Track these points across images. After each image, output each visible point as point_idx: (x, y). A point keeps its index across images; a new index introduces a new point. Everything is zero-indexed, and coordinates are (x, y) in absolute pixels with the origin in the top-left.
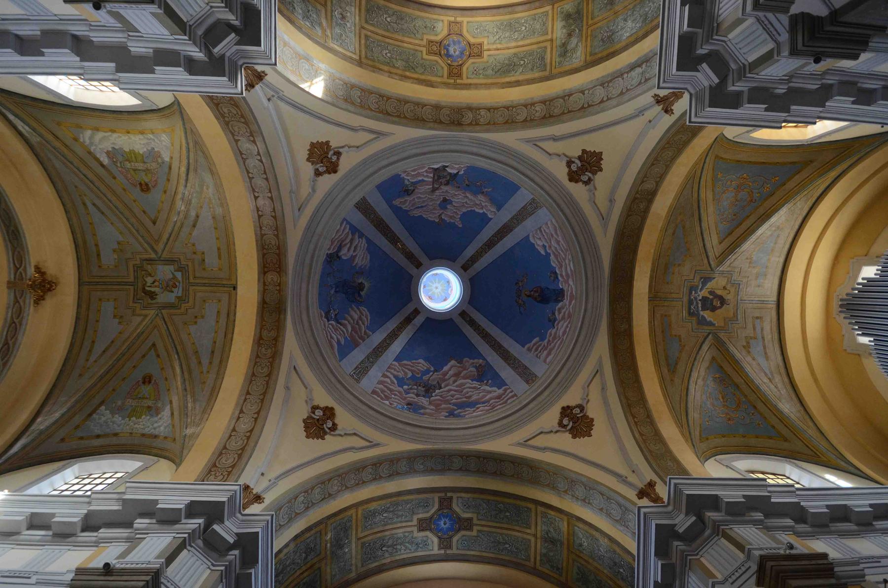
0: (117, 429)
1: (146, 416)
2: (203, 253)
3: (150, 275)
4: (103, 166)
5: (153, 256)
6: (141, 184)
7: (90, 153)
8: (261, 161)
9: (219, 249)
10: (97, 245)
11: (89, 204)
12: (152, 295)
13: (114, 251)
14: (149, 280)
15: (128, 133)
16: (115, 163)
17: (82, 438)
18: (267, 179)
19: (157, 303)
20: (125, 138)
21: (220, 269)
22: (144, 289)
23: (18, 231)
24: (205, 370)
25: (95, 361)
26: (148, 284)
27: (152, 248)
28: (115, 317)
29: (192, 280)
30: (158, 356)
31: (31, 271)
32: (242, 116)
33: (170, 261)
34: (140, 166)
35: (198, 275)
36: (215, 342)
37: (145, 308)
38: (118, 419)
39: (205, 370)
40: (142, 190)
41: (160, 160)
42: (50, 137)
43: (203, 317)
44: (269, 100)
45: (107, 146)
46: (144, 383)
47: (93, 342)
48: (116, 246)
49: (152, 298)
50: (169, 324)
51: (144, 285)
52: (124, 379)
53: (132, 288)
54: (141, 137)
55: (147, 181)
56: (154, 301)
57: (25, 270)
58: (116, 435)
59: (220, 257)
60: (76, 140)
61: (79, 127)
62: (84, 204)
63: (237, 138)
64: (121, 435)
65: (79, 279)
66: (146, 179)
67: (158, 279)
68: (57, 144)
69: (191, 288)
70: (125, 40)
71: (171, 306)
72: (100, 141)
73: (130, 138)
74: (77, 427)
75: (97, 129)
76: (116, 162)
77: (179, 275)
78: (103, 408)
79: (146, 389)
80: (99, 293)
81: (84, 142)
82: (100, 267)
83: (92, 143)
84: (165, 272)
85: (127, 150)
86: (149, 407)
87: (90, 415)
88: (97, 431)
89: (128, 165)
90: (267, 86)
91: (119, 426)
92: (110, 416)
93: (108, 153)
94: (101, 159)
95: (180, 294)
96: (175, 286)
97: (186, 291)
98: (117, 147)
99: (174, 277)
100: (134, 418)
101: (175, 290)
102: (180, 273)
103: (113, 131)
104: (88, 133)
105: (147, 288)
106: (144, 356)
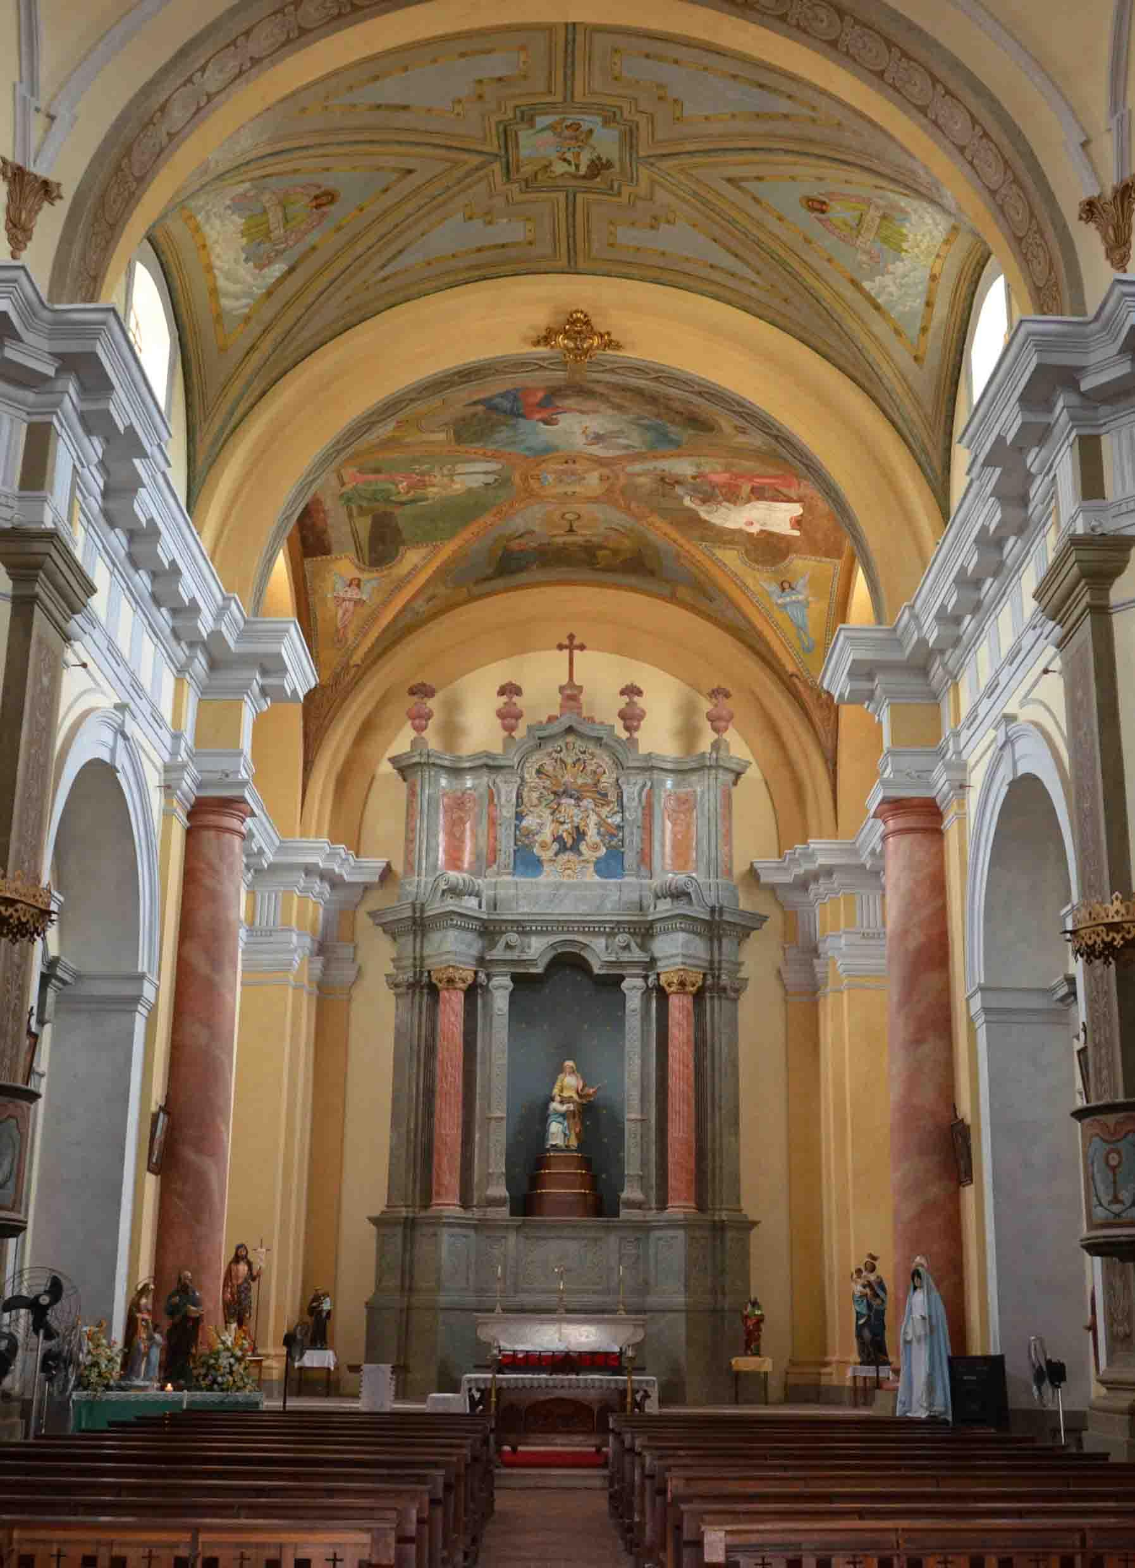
0: (920, 275)
1: (904, 226)
2: (480, 82)
3: (546, 167)
4: (292, 270)
5: (497, 166)
6: (318, 206)
7: (269, 293)
8: (203, 69)
9: (463, 55)
10: (479, 250)
11: (382, 274)
12: (598, 167)
13: (490, 223)
14: (560, 168)
15: (204, 246)
16: (279, 253)
17: (924, 330)
18: (247, 33)
19: (621, 159)
20: (218, 249)
21: (523, 48)
22: (584, 177)
23: (460, 372)
24: (806, 112)
25: (758, 273)
26: (572, 169)
27: (477, 169)
28: (652, 227)
29: (559, 98)
30: (759, 179)
31: (542, 350)
32: (119, 168)
33: (507, 137)
34: (274, 217)
35: (541, 86)
36: (735, 77)
37: (633, 179)
38: (899, 268)
39: (806, 112)
40: (332, 201)
41: (252, 193)
42: (255, 359)
43: (660, 86)
44: (52, 118)
45: (245, 271)
46: (823, 212)
47: (712, 266)
48: (478, 223)
49: (609, 165)
50: (680, 148)
51: (574, 177)
52: (807, 241)
53: (580, 198)
54: (206, 228)
55: (307, 200)
56: (617, 165)
57: (544, 359)
58: (933, 278)
59: (489, 51)
60: (247, 319)
61: (218, 318)
62: (385, 279)
63: (165, 139)
64: (936, 271)
65: (563, 273)
66: (301, 205)
67: (553, 155)
68: (266, 346)
69: (578, 97)
70: (93, 469)
71: (630, 138)
72: (236, 281)
73: (216, 242)
74: (897, 332)
75: (214, 291)
76: (277, 251)
77: (542, 121)
78: (867, 285)
79: (838, 212)
80: (596, 245)
81: (247, 305)
82: (530, 243)
83: (248, 294)
84: (535, 145)
85: (244, 241)
86: (884, 217)
87: (877, 307)
88: (918, 303)
89: (278, 233)
90: (25, 139)
91: (915, 269)
92: (888, 279)
93: (261, 267)
94: (278, 274)
95: (599, 119)
96: (576, 127)
97: (585, 108)
98: (244, 256)
99: (551, 127)
100: (905, 246)
101: (585, 127)
102: (538, 119)
103: (209, 268)
104: (226, 303)
105: (583, 170)
106: (756, 200)
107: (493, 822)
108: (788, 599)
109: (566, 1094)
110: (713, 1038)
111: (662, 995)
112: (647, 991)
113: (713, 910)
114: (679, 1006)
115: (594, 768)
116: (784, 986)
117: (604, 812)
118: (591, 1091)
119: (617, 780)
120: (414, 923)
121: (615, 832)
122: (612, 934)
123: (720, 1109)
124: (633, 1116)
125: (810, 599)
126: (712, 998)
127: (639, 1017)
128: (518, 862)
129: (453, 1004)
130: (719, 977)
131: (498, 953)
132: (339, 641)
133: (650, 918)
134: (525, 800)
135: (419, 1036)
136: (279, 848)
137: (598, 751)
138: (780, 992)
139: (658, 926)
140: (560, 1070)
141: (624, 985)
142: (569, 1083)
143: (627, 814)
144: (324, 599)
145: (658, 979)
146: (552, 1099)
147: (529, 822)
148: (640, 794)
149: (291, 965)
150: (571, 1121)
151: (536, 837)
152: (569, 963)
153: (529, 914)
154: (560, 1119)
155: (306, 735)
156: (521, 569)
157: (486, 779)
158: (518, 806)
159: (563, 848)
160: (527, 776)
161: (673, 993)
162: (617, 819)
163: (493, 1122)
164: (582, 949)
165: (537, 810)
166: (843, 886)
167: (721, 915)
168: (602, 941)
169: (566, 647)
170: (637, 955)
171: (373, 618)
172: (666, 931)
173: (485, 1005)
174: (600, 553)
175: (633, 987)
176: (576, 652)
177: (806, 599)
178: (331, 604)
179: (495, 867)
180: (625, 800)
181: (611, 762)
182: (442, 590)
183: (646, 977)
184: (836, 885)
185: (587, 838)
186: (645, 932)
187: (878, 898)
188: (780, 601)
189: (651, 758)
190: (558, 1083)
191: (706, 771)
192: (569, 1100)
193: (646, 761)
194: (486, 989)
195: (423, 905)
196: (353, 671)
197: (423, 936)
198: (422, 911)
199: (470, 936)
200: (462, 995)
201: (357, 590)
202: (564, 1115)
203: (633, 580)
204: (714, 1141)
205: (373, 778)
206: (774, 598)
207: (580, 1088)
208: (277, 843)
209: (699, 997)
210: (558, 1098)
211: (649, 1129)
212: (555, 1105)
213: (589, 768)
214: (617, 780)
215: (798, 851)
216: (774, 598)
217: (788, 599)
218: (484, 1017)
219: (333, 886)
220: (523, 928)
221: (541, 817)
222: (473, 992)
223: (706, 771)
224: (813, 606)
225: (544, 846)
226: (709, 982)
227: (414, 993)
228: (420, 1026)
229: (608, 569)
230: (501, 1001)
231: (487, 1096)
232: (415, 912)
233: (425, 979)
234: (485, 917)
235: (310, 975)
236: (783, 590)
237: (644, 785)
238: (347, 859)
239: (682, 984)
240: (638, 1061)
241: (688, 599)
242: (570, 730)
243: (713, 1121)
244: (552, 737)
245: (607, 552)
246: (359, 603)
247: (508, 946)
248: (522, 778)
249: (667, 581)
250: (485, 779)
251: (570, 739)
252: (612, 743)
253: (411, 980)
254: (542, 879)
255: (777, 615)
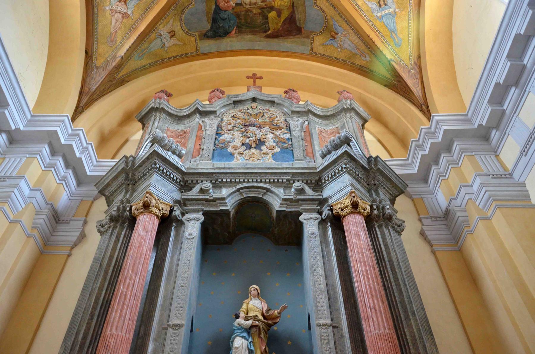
107: (199, 138)
108: (383, 12)
109: (251, 314)
110: (389, 254)
111: (336, 221)
112: (322, 223)
113: (369, 159)
114: (355, 227)
115: (270, 115)
116: (429, 243)
117: (278, 132)
118: (276, 312)
119: (286, 120)
120: (127, 178)
121: (287, 142)
122: (288, 186)
123: (413, 313)
124: (322, 321)
125: (397, 10)
126: (380, 227)
127: (318, 239)
128: (216, 155)
129: (147, 226)
130: (383, 208)
131: (194, 193)
132: (112, 41)
133: (318, 170)
134: (223, 128)
135: (111, 257)
136: (29, 121)
137: (272, 109)
138: (426, 248)
139: (326, 175)
140: (246, 296)
141: (301, 218)
142: (255, 305)
143: (293, 133)
144: (104, 10)
145: (332, 210)
146: (237, 317)
147: (226, 137)
148: (302, 127)
149: (10, 197)
150: (257, 340)
151: (230, 144)
152: (252, 206)
153: (220, 169)
154: (245, 334)
155: (81, 93)
156: (226, 34)
157: (197, 120)
158: (217, 130)
159: (249, 147)
160: (225, 119)
161: (349, 214)
162: (288, 136)
163: (170, 331)
164: (265, 193)
165: (232, 131)
166: (462, 151)
167: (376, 165)
168: (280, 192)
169: (251, 78)
170: (310, 193)
171: (133, 28)
172: (333, 177)
173: (177, 235)
174: (272, 15)
175: (310, 225)
176: (257, 80)
177: (395, 11)
178: (108, 14)
179: (198, 158)
180: (292, 127)
181: (280, 114)
182: (178, 29)
183: (320, 213)
184: (455, 157)
185: (267, 144)
186: (317, 181)
187: (493, 157)
188: (379, 15)
189: (307, 105)
190: (244, 306)
191: (343, 114)
192: (255, 318)
193: (304, 108)
194: (180, 223)
195: (134, 158)
196: (119, 59)
197: (134, 191)
198: (133, 162)
199: (171, 186)
200: (157, 222)
201: (124, 6)
202: (249, 330)
203: (287, 44)
204: (415, 344)
205: (127, 141)
206: (375, 13)
207: (265, 309)
208: (29, 117)
209: (369, 220)
210: (242, 315)
211: (342, 336)
212: (241, 321)
213: (266, 116)
214: (286, 120)
215: (423, 130)
216: (375, 13)
217: (383, 12)
218: (175, 244)
219: (79, 183)
220: (216, 179)
221: (232, 135)
222: (167, 223)
223: (343, 114)
224: (398, 15)
225: (235, 148)
226: (376, 212)
227: (115, 227)
228: (114, 249)
229: (275, 36)
230: (193, 228)
231: (168, 308)
232: (127, 163)
233: (127, 213)
234: (185, 171)
235: (33, 224)
236: (380, 6)
237: (304, 123)
238: (87, 148)
239: (355, 205)
240: (320, 271)
241: (321, 50)
242: (254, 100)
243: (410, 326)
244: (240, 102)
245: (272, 15)
246: (125, 16)
247: (202, 191)
248: (222, 119)
249: (308, 37)
250: (197, 119)
251: (254, 105)
252: (280, 102)
253: (114, 213)
254: (233, 162)
255: (377, 24)
